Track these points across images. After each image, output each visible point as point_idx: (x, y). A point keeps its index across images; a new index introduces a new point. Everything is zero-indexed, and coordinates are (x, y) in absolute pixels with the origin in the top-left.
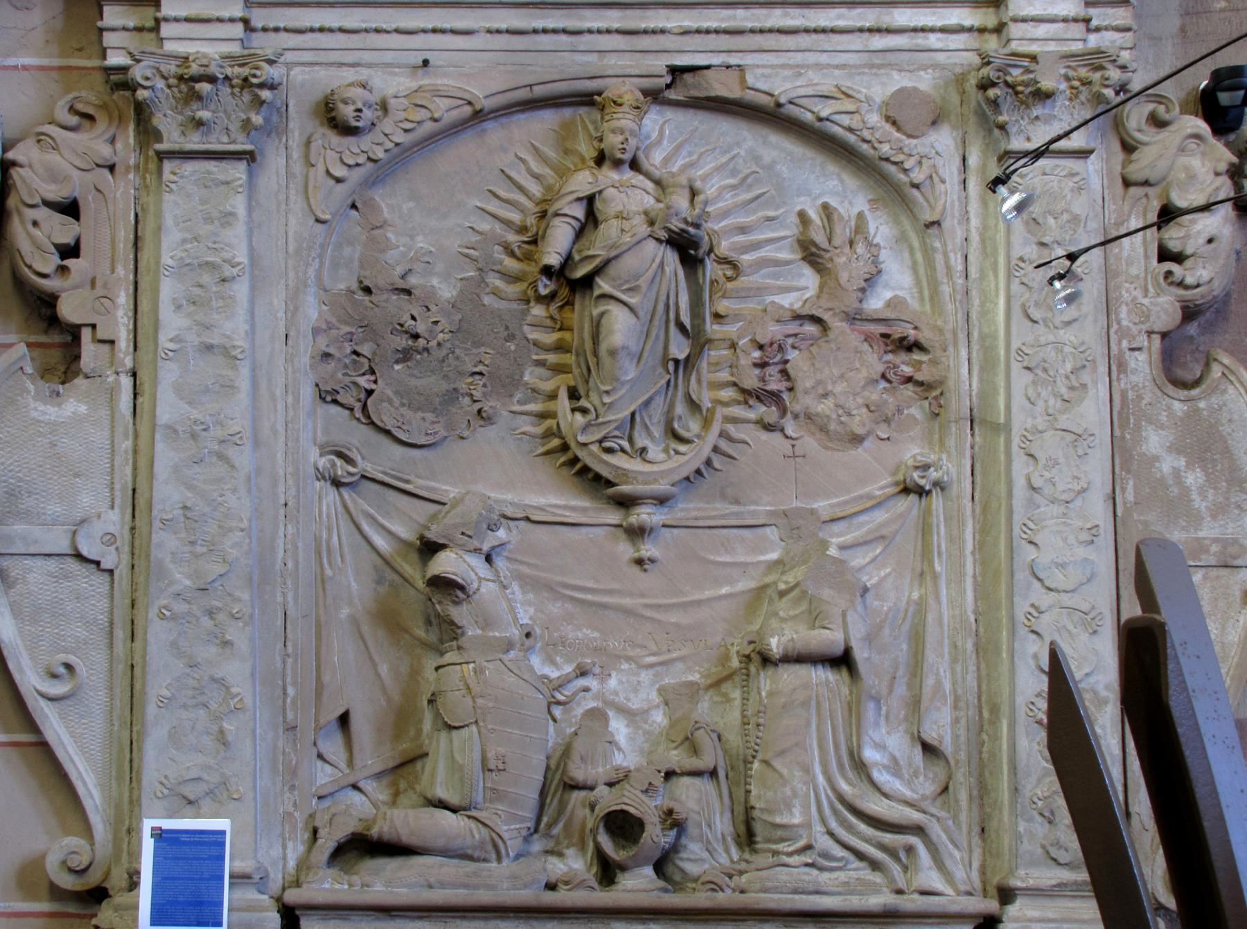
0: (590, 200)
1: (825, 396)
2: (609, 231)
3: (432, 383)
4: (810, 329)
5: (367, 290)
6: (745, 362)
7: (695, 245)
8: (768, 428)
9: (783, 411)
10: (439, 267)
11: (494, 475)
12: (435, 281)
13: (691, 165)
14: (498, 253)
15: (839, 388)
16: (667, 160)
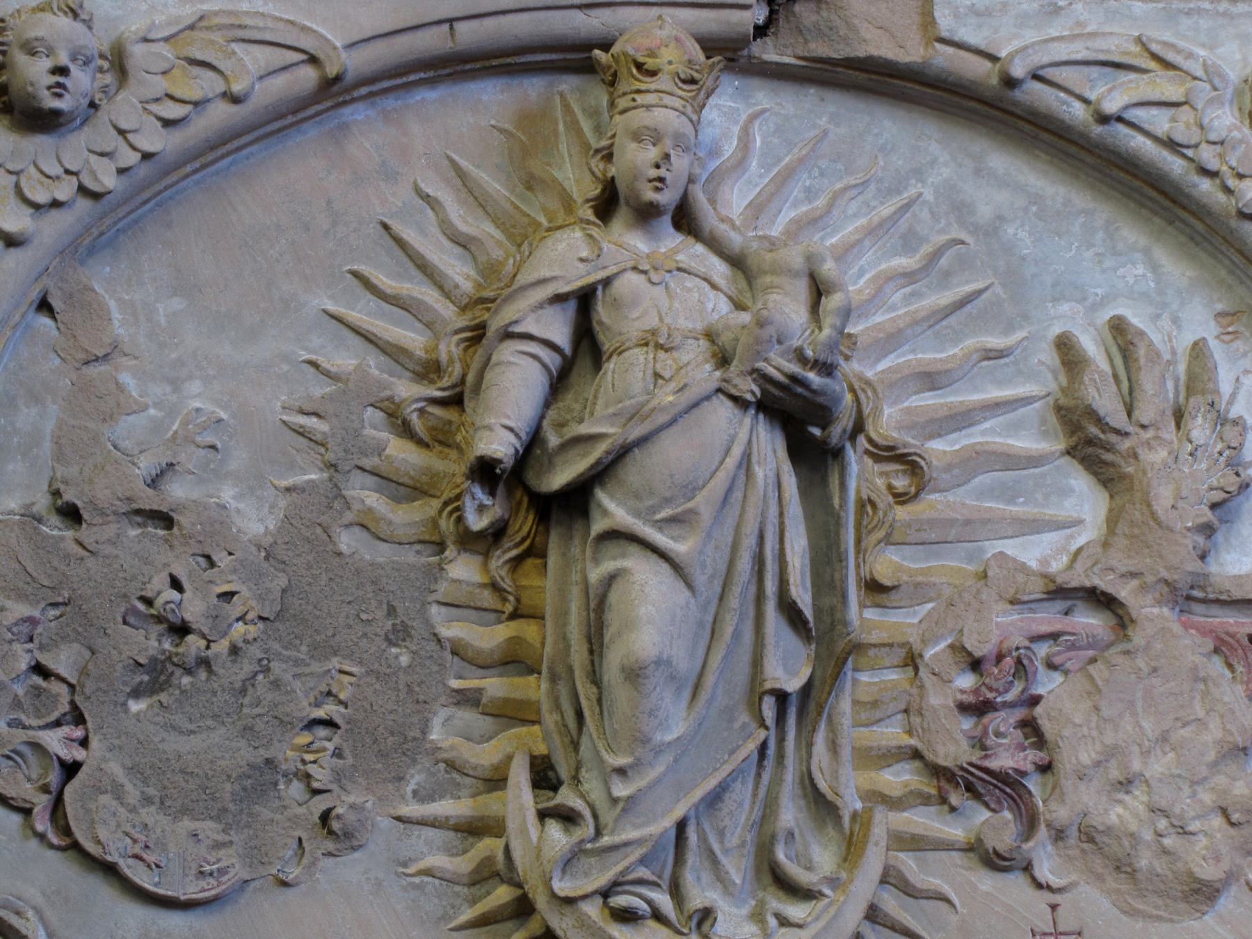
0: (585, 300)
1: (1126, 784)
2: (626, 374)
3: (215, 747)
4: (1089, 621)
5: (72, 514)
6: (938, 699)
7: (823, 413)
8: (996, 862)
9: (1030, 822)
10: (238, 459)
12: (227, 494)
14: (374, 427)
15: (1158, 766)
16: (757, 209)
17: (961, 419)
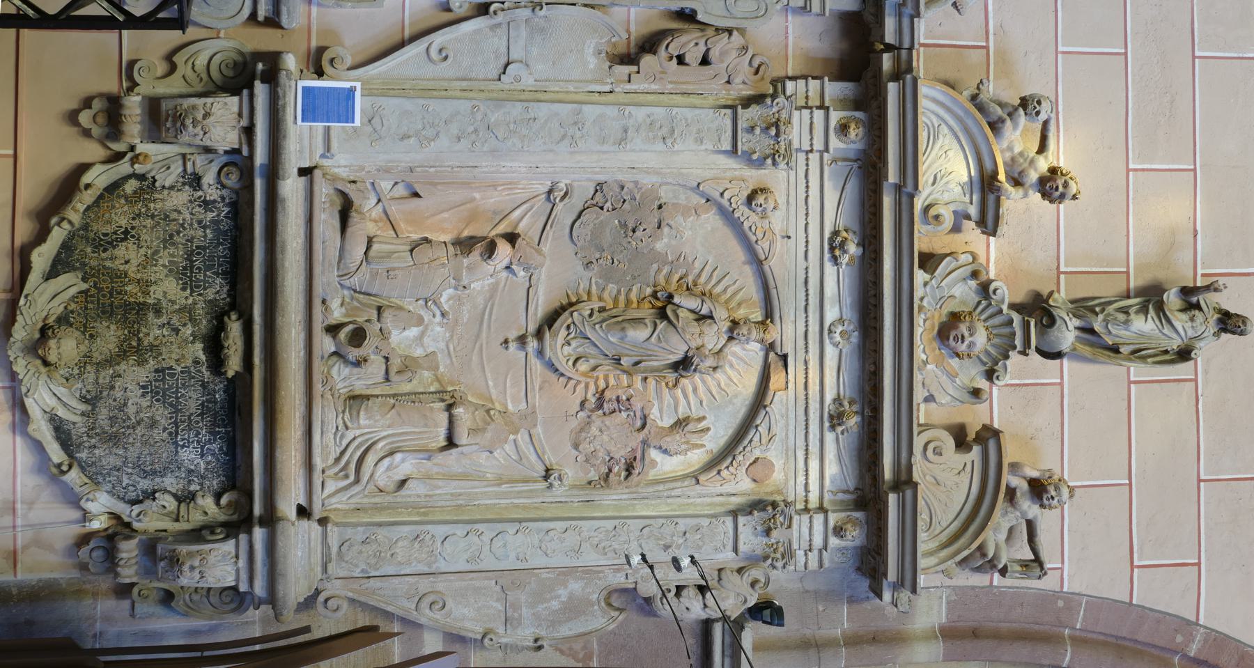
0: (711, 317)
1: (601, 431)
3: (607, 238)
4: (639, 423)
5: (660, 207)
6: (620, 392)
7: (685, 369)
8: (583, 403)
9: (592, 411)
10: (674, 242)
11: (556, 271)
12: (666, 240)
13: (731, 366)
14: (682, 271)
15: (605, 438)
16: (734, 354)
17: (686, 396)
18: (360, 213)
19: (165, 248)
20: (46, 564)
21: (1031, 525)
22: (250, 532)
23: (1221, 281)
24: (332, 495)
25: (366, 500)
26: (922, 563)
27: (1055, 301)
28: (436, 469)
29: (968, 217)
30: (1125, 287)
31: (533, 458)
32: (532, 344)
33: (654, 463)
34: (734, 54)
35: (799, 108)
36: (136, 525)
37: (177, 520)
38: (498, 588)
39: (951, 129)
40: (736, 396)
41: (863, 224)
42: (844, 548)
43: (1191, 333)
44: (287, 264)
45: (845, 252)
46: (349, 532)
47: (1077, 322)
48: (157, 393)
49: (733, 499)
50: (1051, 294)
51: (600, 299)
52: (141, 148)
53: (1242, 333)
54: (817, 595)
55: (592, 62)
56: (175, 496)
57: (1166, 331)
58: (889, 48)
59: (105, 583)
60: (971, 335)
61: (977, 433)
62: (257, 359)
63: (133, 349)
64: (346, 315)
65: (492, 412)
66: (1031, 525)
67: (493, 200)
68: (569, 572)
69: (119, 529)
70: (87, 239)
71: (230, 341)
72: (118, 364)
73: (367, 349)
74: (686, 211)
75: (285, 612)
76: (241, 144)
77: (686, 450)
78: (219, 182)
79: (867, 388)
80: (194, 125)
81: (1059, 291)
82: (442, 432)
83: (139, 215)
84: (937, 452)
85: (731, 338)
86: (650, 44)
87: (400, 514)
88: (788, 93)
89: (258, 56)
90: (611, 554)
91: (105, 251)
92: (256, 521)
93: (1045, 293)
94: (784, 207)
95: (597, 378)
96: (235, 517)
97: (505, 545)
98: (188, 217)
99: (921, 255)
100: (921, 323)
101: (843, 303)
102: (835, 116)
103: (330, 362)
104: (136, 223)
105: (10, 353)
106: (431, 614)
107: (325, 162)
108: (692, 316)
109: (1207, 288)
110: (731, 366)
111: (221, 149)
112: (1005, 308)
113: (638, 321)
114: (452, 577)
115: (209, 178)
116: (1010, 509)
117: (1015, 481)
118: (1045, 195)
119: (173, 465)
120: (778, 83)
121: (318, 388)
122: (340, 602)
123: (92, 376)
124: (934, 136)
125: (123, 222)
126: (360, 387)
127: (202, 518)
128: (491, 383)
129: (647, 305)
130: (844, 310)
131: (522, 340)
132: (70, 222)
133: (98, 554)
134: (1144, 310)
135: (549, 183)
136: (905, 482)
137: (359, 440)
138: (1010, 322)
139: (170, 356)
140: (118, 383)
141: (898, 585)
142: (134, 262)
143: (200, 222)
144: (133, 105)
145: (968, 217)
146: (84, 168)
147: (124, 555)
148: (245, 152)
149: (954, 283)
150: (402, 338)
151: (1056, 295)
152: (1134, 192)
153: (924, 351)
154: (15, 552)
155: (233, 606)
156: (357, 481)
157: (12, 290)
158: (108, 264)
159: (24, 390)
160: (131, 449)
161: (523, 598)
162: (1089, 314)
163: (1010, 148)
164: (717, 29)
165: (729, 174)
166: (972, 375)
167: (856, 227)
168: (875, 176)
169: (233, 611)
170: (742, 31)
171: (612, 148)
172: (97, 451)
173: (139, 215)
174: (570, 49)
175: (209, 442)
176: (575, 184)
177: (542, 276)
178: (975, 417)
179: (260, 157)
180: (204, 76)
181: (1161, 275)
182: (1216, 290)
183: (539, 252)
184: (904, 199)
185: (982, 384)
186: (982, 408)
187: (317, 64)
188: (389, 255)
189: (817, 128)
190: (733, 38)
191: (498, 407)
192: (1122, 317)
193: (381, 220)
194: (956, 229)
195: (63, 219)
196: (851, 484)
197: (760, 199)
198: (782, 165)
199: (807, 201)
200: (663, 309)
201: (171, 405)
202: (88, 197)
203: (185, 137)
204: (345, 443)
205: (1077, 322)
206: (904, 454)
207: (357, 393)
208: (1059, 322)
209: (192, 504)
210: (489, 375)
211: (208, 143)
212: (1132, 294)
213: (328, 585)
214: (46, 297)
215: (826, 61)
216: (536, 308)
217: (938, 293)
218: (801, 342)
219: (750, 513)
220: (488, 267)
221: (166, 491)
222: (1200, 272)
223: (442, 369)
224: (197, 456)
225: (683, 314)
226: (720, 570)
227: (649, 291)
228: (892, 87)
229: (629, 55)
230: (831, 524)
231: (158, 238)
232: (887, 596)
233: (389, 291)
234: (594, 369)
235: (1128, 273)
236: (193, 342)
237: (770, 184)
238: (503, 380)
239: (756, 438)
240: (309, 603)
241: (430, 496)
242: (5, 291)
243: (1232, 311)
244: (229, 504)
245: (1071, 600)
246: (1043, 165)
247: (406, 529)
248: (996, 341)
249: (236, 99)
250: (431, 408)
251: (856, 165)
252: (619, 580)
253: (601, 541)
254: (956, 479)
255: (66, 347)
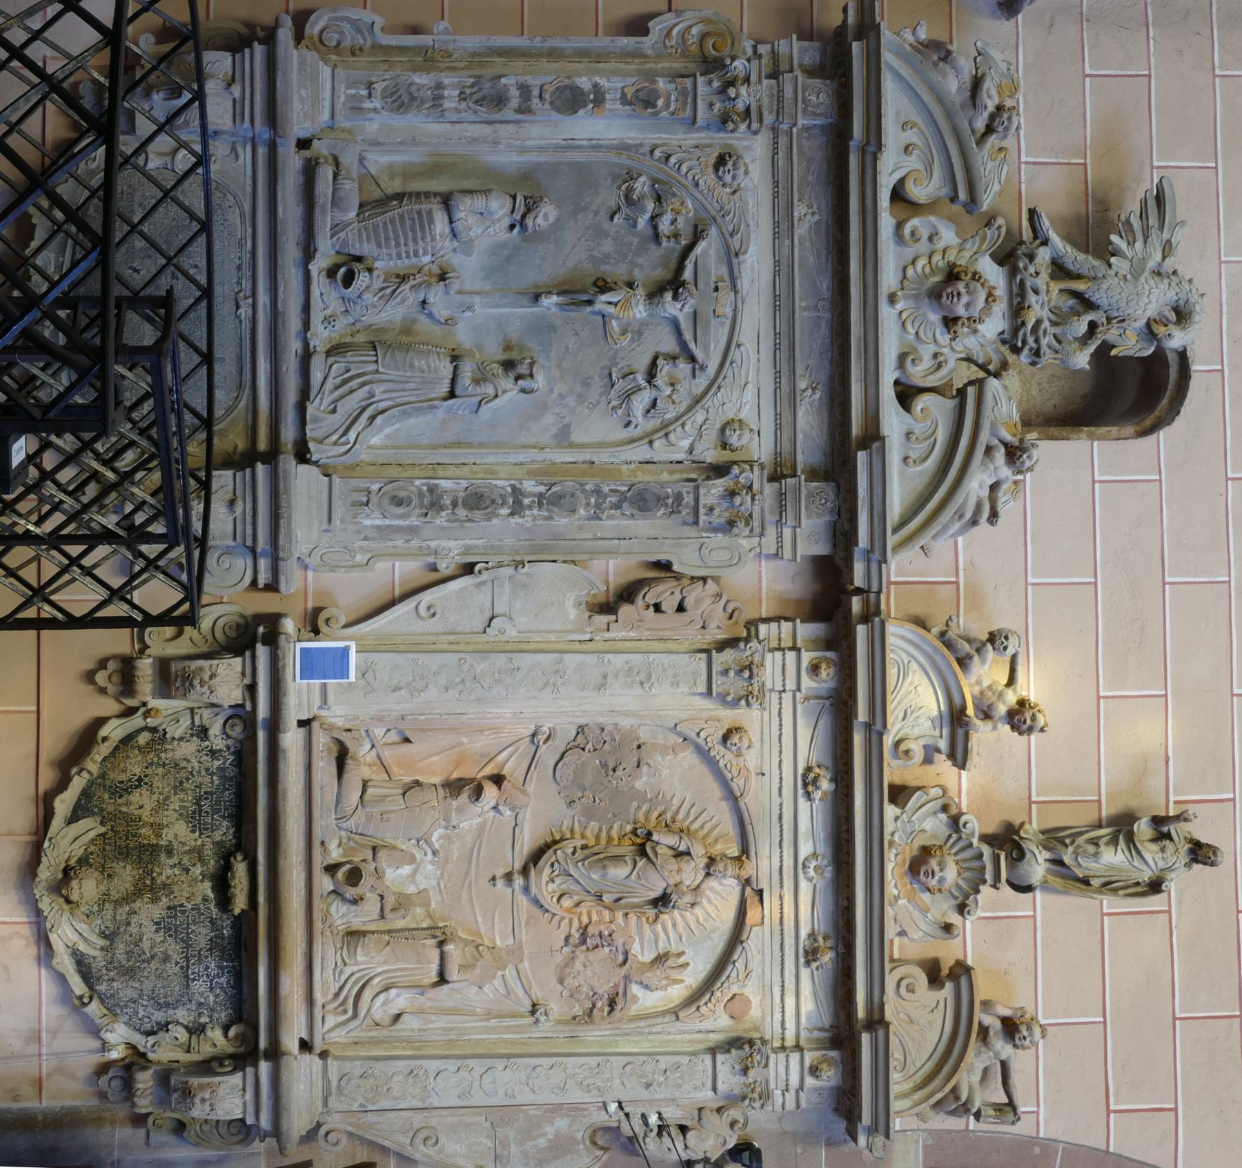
0: (689, 854)
1: (584, 966)
2: (673, 865)
3: (589, 777)
4: (621, 959)
5: (639, 747)
6: (602, 928)
7: (665, 905)
8: (567, 939)
9: (576, 946)
10: (653, 780)
11: (540, 810)
12: (645, 779)
13: (709, 901)
14: (661, 808)
15: (589, 973)
16: (712, 889)
17: (666, 932)
18: (355, 760)
19: (176, 793)
20: (68, 1092)
21: (1004, 1065)
22: (256, 1066)
23: (1192, 809)
24: (332, 1029)
25: (363, 1034)
26: (895, 1105)
27: (1026, 832)
28: (428, 1004)
29: (938, 751)
30: (1096, 816)
31: (520, 992)
32: (519, 881)
33: (635, 999)
34: (709, 601)
35: (772, 650)
36: (151, 1056)
37: (188, 1051)
38: (488, 1124)
39: (921, 665)
40: (714, 931)
41: (835, 759)
42: (821, 1088)
43: (1161, 864)
44: (288, 810)
45: (818, 788)
46: (348, 1066)
47: (1047, 855)
48: (170, 929)
49: (712, 1036)
50: (1022, 824)
51: (583, 836)
52: (153, 703)
53: (1212, 864)
54: (796, 1137)
55: (573, 613)
56: (186, 1027)
57: (1136, 863)
58: (858, 591)
59: (122, 1111)
60: (941, 870)
61: (951, 969)
62: (261, 899)
63: (147, 888)
64: (344, 855)
65: (481, 948)
66: (1004, 1065)
67: (481, 743)
68: (554, 1110)
69: (135, 1058)
70: (105, 786)
71: (237, 881)
72: (134, 902)
73: (364, 888)
74: (664, 750)
75: (289, 1146)
76: (244, 700)
77: (666, 986)
78: (225, 733)
79: (841, 923)
80: (202, 683)
81: (1030, 822)
82: (434, 968)
83: (151, 764)
84: (911, 990)
85: (708, 875)
86: (628, 593)
87: (395, 1048)
88: (761, 638)
89: (259, 618)
90: (594, 1092)
91: (121, 797)
92: (261, 1054)
93: (1017, 823)
94: (759, 745)
95: (581, 914)
96: (242, 1049)
97: (494, 1082)
98: (196, 765)
99: (892, 787)
100: (893, 858)
101: (817, 838)
102: (807, 657)
103: (329, 900)
104: (149, 771)
105: (35, 891)
106: (425, 1150)
107: (323, 713)
108: (671, 852)
109: (1177, 818)
110: (709, 901)
111: (226, 705)
112: (975, 841)
113: (618, 858)
114: (444, 1112)
115: (215, 730)
116: (983, 1049)
117: (988, 1020)
118: (1014, 728)
119: (185, 996)
120: (752, 624)
121: (318, 925)
122: (340, 1136)
123: (110, 912)
124: (903, 672)
125: (137, 771)
126: (357, 923)
127: (211, 1050)
128: (479, 919)
129: (627, 842)
130: (818, 844)
131: (508, 877)
132: (89, 772)
133: (116, 1083)
134: (1114, 841)
135: (533, 727)
136: (877, 1022)
137: (357, 975)
138: (980, 856)
139: (181, 894)
140: (134, 920)
141: (872, 1130)
142: (148, 807)
143: (207, 770)
144: (145, 667)
145: (938, 751)
146: (100, 722)
147: (140, 1086)
148: (248, 707)
149: (925, 817)
150: (396, 876)
151: (1027, 826)
152: (1106, 719)
153: (896, 886)
154: (40, 1080)
155: (240, 1137)
156: (355, 1016)
157: (36, 833)
158: (124, 809)
159: (48, 926)
160: (146, 982)
161: (512, 1135)
162: (1059, 846)
163: (979, 683)
164: (692, 578)
165: (705, 715)
166: (943, 909)
167: (828, 762)
168: (847, 712)
169: (240, 1142)
170: (716, 579)
171: (592, 694)
172: (115, 984)
173: (151, 764)
174: (551, 601)
175: (218, 976)
176: (558, 727)
177: (527, 815)
178: (948, 953)
179: (263, 712)
180: (210, 638)
181: (1133, 803)
182: (1186, 820)
183: (524, 793)
184: (874, 737)
185: (954, 918)
186: (955, 943)
187: (313, 624)
188: (383, 798)
189: (789, 671)
190: (708, 586)
191: (487, 942)
192: (1091, 849)
193: (375, 764)
194: (928, 760)
195: (82, 769)
196: (827, 1021)
197: (735, 739)
198: (756, 706)
199: (781, 736)
200: (642, 846)
201: (182, 940)
202: (104, 750)
203: (193, 695)
204: (343, 978)
205: (1047, 855)
206: (877, 993)
207: (354, 928)
208: (1028, 855)
209: (202, 1037)
210: (477, 911)
211: (215, 701)
212: (1104, 823)
213: (329, 1119)
214: (68, 841)
215: (799, 602)
216: (522, 846)
217: (907, 827)
218: (776, 878)
219: (728, 1051)
220: (477, 808)
221: (178, 1023)
222: (1172, 799)
223: (433, 905)
224: (208, 987)
225: (660, 850)
226: (700, 1110)
227: (629, 828)
228: (861, 630)
229: (608, 604)
230: (807, 1063)
231: (169, 785)
232: (862, 1140)
233: (384, 834)
234: (577, 905)
235: (1099, 801)
236: (202, 881)
237: (744, 723)
238: (492, 917)
239: (734, 975)
240: (311, 1135)
241: (424, 1030)
242: (30, 834)
243: (1203, 841)
244: (237, 1036)
245: (1048, 1146)
246: (1011, 698)
247: (401, 1064)
248: (968, 874)
249: (239, 660)
250: (424, 945)
251: (827, 703)
252: (601, 1118)
253: (585, 1078)
254: (930, 1017)
255: (87, 888)
